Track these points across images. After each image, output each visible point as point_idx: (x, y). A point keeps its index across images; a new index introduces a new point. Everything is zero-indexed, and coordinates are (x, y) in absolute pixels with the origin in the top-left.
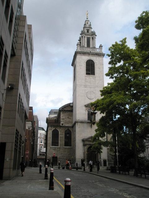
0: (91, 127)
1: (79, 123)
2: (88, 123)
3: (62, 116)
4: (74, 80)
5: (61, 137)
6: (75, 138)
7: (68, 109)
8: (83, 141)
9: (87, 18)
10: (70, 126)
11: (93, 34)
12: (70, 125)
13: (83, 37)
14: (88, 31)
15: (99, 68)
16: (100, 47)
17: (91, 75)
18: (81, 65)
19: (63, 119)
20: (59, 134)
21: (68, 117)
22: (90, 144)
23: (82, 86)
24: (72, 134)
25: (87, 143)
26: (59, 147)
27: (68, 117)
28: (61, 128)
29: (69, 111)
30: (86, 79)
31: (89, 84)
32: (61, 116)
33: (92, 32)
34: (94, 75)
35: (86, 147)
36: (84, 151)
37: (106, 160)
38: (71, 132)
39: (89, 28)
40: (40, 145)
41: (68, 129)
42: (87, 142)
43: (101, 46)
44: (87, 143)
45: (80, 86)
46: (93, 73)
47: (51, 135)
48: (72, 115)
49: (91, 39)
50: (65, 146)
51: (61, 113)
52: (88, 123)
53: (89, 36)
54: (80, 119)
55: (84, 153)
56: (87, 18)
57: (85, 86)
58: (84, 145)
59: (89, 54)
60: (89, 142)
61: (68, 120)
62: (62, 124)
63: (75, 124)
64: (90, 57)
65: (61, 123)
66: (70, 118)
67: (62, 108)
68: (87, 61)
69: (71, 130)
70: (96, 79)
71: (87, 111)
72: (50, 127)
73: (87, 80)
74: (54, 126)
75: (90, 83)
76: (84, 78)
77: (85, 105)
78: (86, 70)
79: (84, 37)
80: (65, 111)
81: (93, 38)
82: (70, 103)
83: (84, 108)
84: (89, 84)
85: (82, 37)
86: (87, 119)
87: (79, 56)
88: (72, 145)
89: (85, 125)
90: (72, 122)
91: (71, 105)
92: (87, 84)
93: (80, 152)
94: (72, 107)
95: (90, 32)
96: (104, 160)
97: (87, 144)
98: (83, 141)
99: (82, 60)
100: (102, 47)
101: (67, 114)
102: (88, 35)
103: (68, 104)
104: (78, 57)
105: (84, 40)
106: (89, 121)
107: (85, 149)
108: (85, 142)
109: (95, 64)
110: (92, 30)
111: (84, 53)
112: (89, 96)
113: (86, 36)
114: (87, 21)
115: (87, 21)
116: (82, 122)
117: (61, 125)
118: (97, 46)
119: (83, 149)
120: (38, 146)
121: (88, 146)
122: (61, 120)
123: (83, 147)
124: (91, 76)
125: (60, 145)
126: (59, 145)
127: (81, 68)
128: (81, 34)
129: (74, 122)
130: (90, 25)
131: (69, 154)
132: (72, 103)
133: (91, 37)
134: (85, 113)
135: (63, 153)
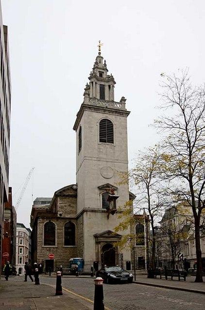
0: (108, 219)
2: (103, 212)
3: (60, 202)
4: (79, 151)
6: (82, 233)
7: (68, 194)
8: (96, 237)
9: (100, 53)
11: (111, 79)
13: (94, 83)
14: (101, 75)
15: (121, 134)
16: (121, 101)
18: (92, 127)
19: (62, 207)
21: (70, 205)
22: (106, 242)
23: (93, 159)
24: (76, 228)
25: (101, 239)
27: (70, 205)
28: (59, 220)
29: (71, 196)
31: (105, 157)
33: (109, 77)
34: (113, 143)
35: (99, 246)
39: (103, 69)
40: (19, 246)
41: (70, 222)
42: (101, 238)
43: (123, 100)
45: (90, 159)
46: (111, 141)
47: (43, 230)
49: (107, 88)
51: (59, 199)
52: (103, 212)
53: (103, 83)
54: (91, 207)
55: (97, 254)
56: (100, 53)
58: (97, 243)
59: (105, 110)
61: (69, 209)
62: (61, 215)
63: (82, 213)
64: (106, 115)
68: (101, 121)
70: (117, 149)
71: (101, 196)
73: (101, 150)
74: (47, 218)
75: (107, 155)
76: (96, 147)
77: (98, 187)
78: (100, 135)
79: (96, 83)
80: (64, 196)
81: (109, 86)
82: (73, 185)
83: (97, 191)
84: (105, 157)
85: (92, 82)
88: (76, 243)
89: (99, 215)
91: (75, 187)
92: (101, 156)
93: (90, 252)
94: (76, 190)
95: (104, 76)
98: (96, 237)
99: (94, 119)
102: (101, 81)
105: (96, 88)
106: (105, 210)
108: (99, 238)
109: (114, 127)
110: (109, 74)
111: (97, 109)
112: (105, 174)
113: (99, 83)
114: (99, 58)
115: (99, 58)
116: (93, 211)
117: (59, 216)
118: (117, 99)
120: (17, 247)
121: (102, 244)
122: (59, 209)
124: (108, 146)
126: (56, 244)
127: (91, 132)
128: (89, 78)
129: (79, 211)
130: (105, 65)
132: (76, 185)
133: (107, 84)
135: (62, 254)
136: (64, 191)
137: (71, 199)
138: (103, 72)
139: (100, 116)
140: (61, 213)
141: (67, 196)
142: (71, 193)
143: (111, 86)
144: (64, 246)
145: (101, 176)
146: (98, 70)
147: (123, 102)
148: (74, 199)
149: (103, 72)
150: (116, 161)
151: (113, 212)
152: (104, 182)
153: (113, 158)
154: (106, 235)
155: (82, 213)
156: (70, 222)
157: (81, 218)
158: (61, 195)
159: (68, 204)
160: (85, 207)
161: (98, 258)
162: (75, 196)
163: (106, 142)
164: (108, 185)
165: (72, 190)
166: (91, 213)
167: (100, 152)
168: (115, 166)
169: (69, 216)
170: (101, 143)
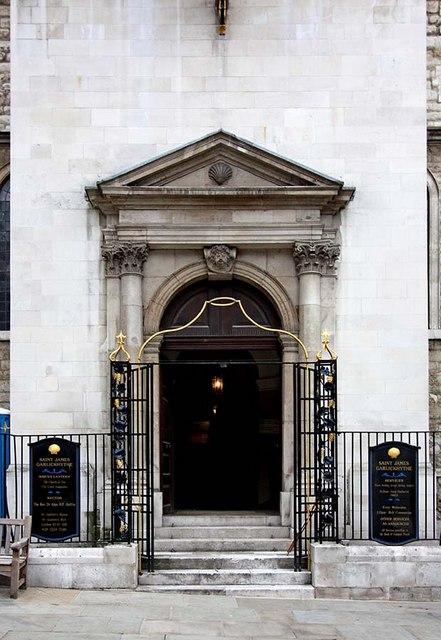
0: (223, 29)
8: (102, 200)
22: (199, 251)
25: (151, 225)
35: (132, 286)
37: (409, 452)
42: (154, 217)
58: (120, 260)
60: (178, 218)
96: (378, 453)
97: (153, 241)
98: (102, 200)
107: (123, 308)
108: (126, 217)
119: (96, 320)
121: (166, 276)
123: (97, 286)
154: (198, 181)
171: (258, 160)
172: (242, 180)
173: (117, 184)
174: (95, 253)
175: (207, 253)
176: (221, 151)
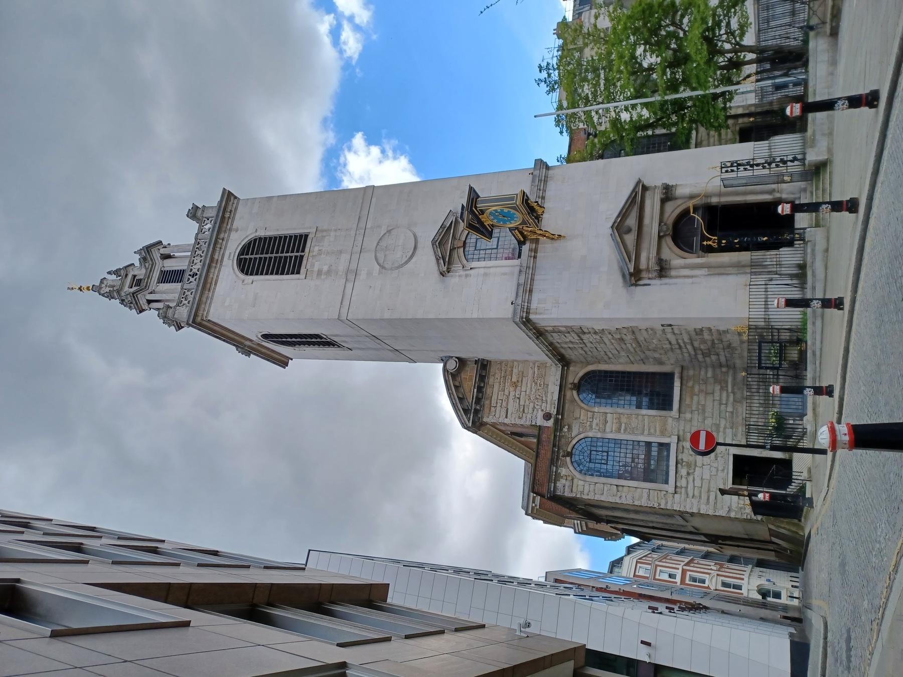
1: (533, 306)
5: (619, 430)
8: (634, 277)
10: (559, 373)
12: (554, 374)
14: (139, 283)
17: (307, 250)
20: (599, 435)
21: (515, 385)
25: (648, 257)
26: (674, 439)
27: (515, 385)
29: (482, 378)
30: (320, 273)
31: (345, 257)
32: (507, 421)
33: (144, 260)
35: (676, 262)
36: (704, 271)
38: (593, 372)
41: (578, 387)
42: (644, 255)
43: (194, 213)
44: (648, 257)
46: (300, 241)
48: (507, 366)
50: (671, 409)
53: (156, 275)
55: (719, 270)
57: (352, 274)
58: (663, 270)
60: (645, 245)
61: (527, 385)
62: (547, 416)
63: (539, 333)
65: (540, 421)
66: (522, 375)
67: (466, 411)
68: (242, 271)
69: (581, 374)
71: (474, 264)
72: (559, 485)
73: (325, 268)
75: (341, 252)
78: (282, 274)
80: (478, 401)
82: (445, 370)
83: (454, 280)
84: (345, 257)
85: (149, 302)
86: (516, 262)
87: (212, 310)
88: (666, 369)
90: (542, 366)
91: (452, 365)
92: (342, 267)
95: (141, 273)
98: (634, 277)
99: (245, 300)
100: (195, 208)
101: (496, 390)
103: (446, 381)
104: (216, 313)
106: (526, 248)
108: (643, 265)
109: (262, 233)
110: (136, 260)
112: (398, 256)
116: (527, 289)
117: (550, 423)
121: (670, 252)
125: (663, 433)
128: (141, 311)
129: (535, 352)
130: (117, 272)
131: (718, 388)
134: (482, 271)
136: (461, 400)
137: (491, 380)
138: (135, 276)
139: (228, 271)
140: (540, 415)
141: (480, 389)
142: (470, 376)
143: (163, 251)
144: (675, 412)
145: (410, 265)
146: (126, 289)
147: (199, 213)
148: (493, 370)
149: (135, 276)
150: (362, 225)
151: (532, 209)
152: (427, 258)
153: (353, 233)
154: (630, 239)
155: (539, 333)
156: (578, 387)
157: (556, 338)
158: (477, 412)
159: (509, 389)
160: (510, 315)
161: (739, 267)
162: (484, 366)
163: (302, 257)
164: (439, 242)
165: (463, 375)
166: (535, 297)
167: (329, 272)
168: (379, 227)
169: (554, 389)
170: (303, 270)
171: (624, 214)
172: (632, 221)
173: (629, 266)
174: (657, 282)
175: (662, 234)
176: (619, 227)
